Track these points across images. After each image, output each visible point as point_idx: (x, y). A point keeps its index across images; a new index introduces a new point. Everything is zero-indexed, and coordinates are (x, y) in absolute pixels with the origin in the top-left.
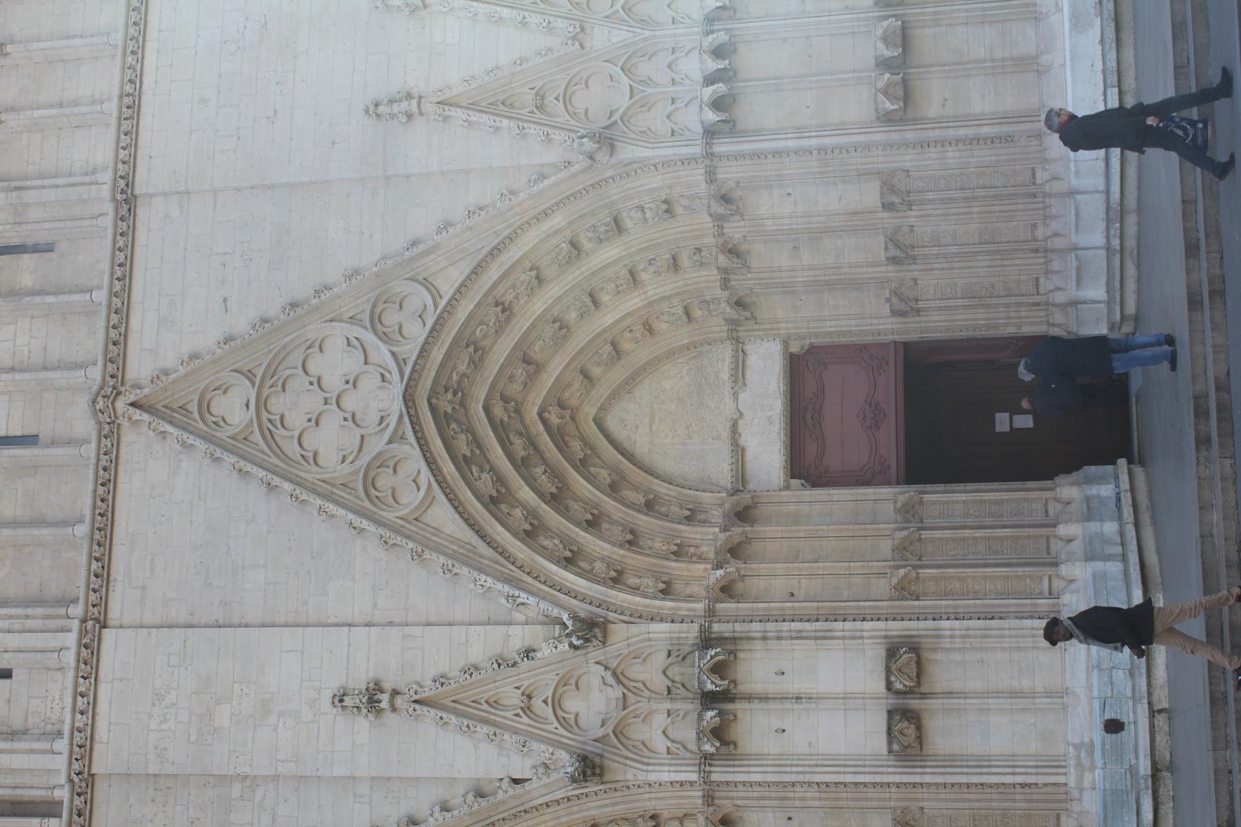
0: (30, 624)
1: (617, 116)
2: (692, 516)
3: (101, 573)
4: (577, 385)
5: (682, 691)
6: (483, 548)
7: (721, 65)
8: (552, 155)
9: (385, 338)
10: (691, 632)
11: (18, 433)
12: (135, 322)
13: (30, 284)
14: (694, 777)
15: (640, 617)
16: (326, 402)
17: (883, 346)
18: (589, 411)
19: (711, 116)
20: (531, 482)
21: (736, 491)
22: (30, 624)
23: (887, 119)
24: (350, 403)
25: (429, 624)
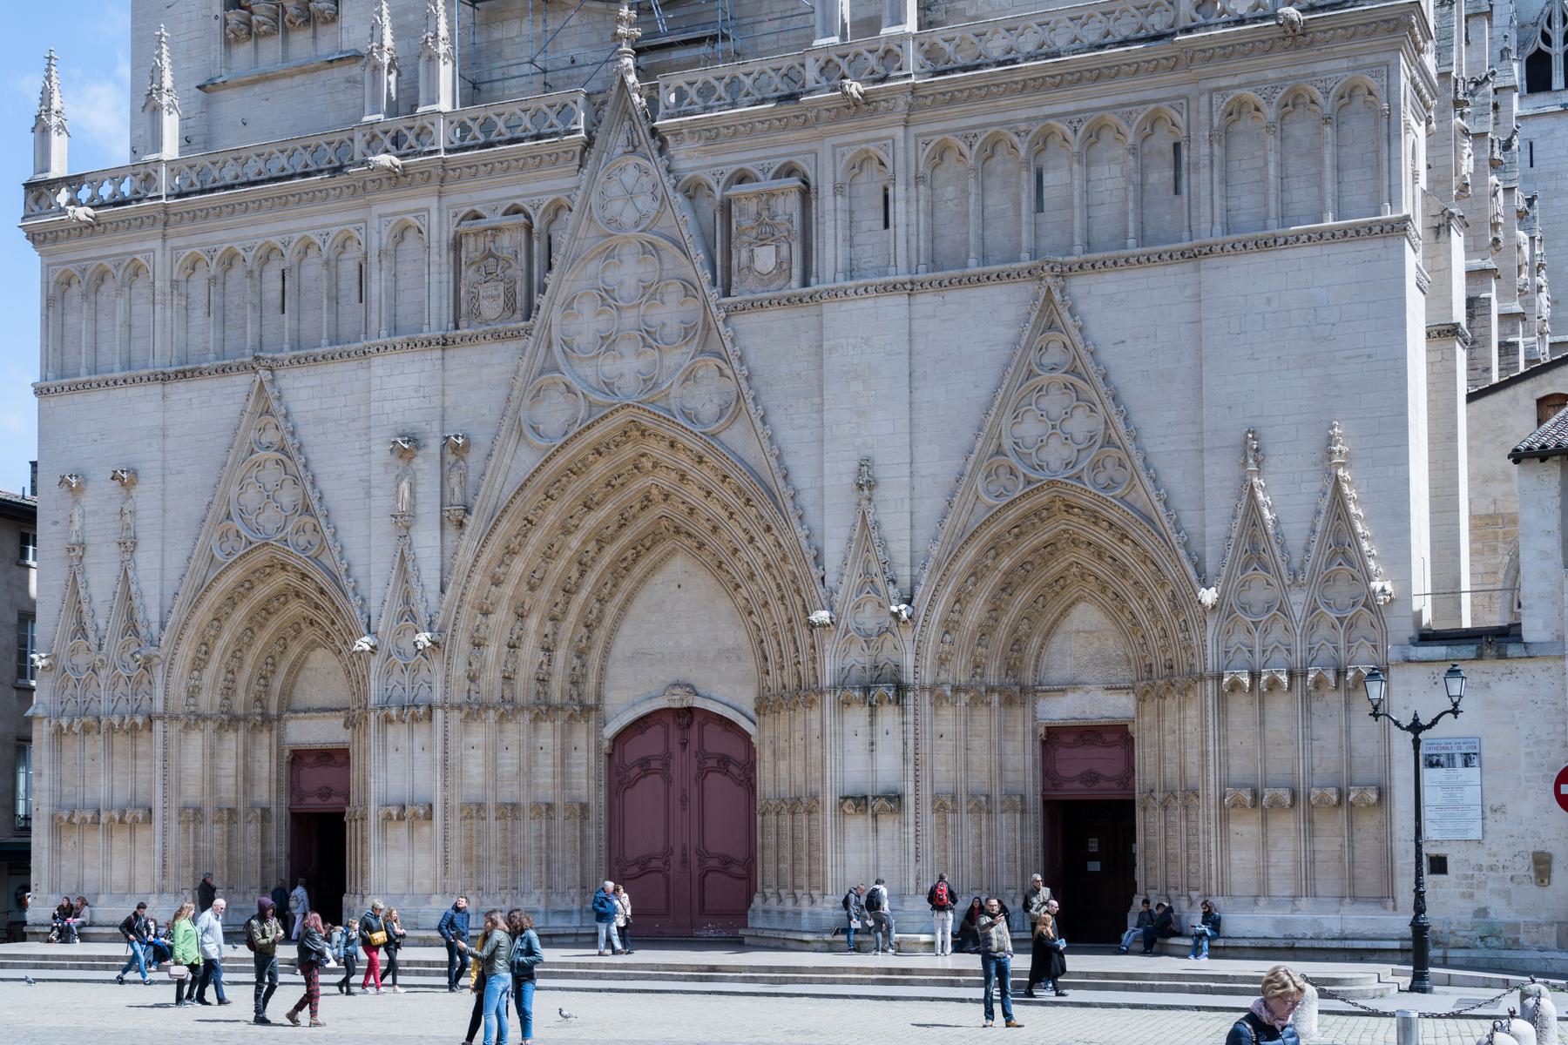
0: (913, 239)
5: (877, 674)
11: (1047, 193)
12: (1110, 276)
13: (1150, 181)
15: (918, 647)
16: (1053, 427)
22: (913, 239)
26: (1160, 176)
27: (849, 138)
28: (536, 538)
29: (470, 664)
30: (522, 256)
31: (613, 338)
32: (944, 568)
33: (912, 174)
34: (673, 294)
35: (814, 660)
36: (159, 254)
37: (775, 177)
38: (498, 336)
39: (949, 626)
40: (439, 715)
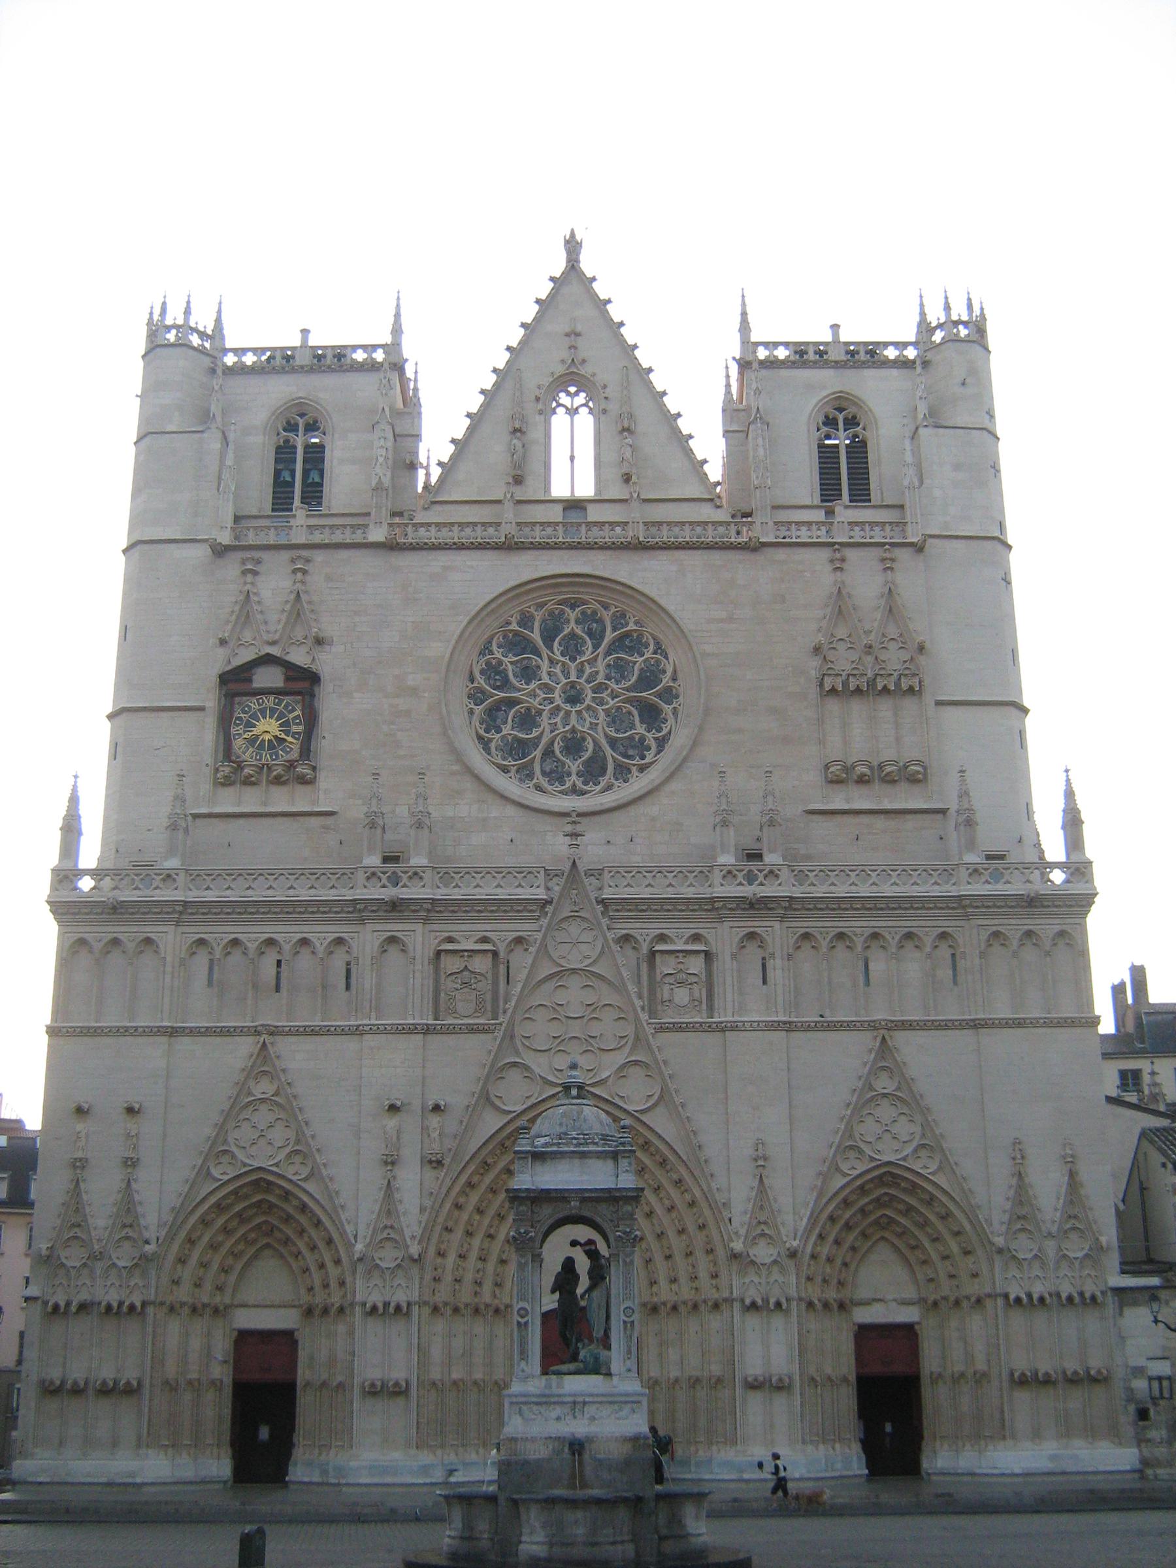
1: (1014, 1253)
2: (841, 1283)
3: (808, 1028)
4: (898, 1229)
6: (824, 1200)
7: (1035, 1302)
8: (996, 1224)
9: (916, 1150)
10: (793, 1292)
11: (871, 974)
12: (920, 1033)
14: (735, 1295)
17: (918, 1368)
18: (887, 1234)
19: (1012, 1297)
20: (854, 1215)
21: (851, 1301)
23: (1012, 1374)
24: (887, 1136)
25: (792, 1178)
26: (945, 973)
27: (742, 924)
28: (488, 1179)
29: (436, 1269)
30: (489, 976)
31: (562, 1038)
32: (814, 1219)
33: (785, 953)
34: (608, 1016)
35: (715, 1276)
36: (170, 937)
37: (686, 943)
38: (473, 1030)
39: (813, 1257)
40: (415, 1309)
